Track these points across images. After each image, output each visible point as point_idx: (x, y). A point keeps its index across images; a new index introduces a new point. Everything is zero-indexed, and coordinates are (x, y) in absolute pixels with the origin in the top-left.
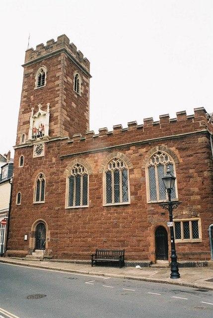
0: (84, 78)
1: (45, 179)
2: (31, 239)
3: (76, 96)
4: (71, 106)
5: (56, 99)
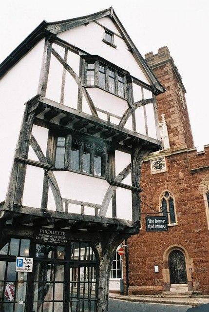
1: (173, 197)
2: (164, 271)
5: (171, 110)
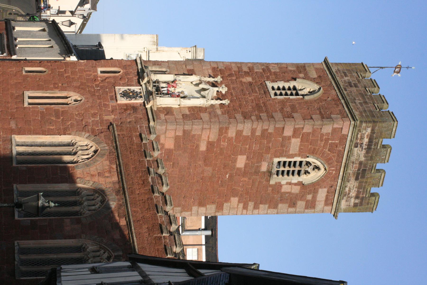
3: (264, 168)
4: (236, 152)
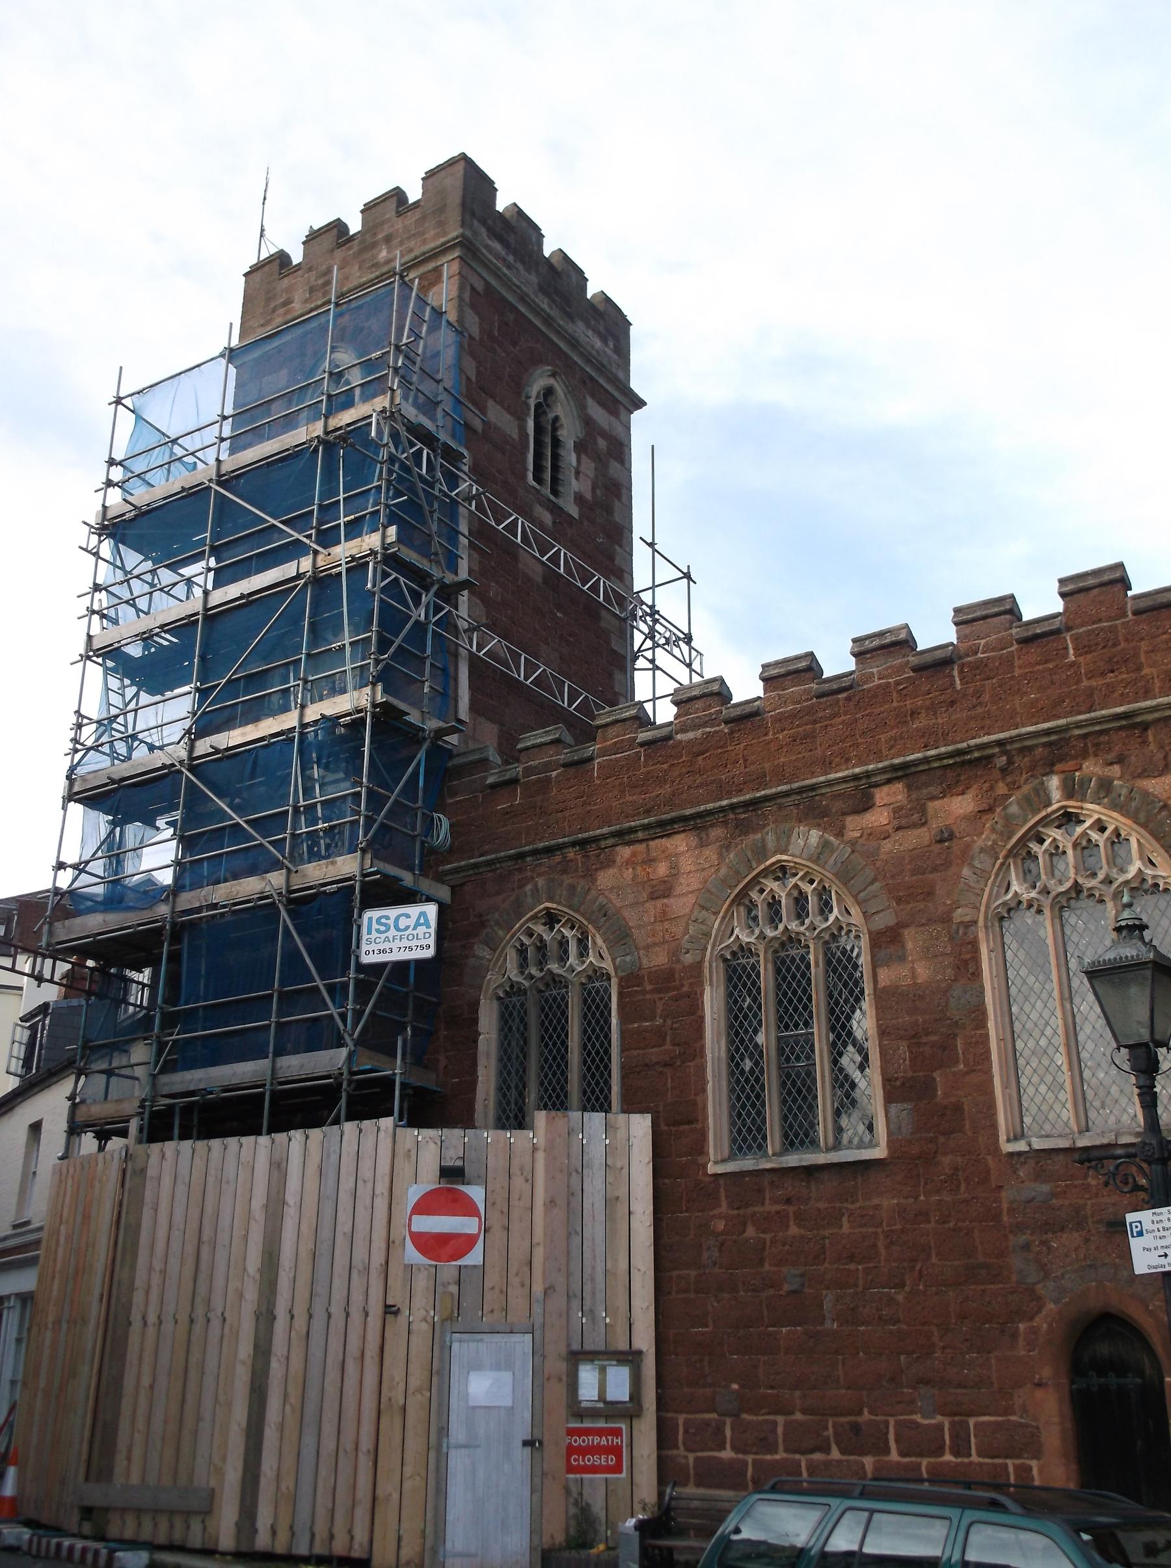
0: (597, 412)
